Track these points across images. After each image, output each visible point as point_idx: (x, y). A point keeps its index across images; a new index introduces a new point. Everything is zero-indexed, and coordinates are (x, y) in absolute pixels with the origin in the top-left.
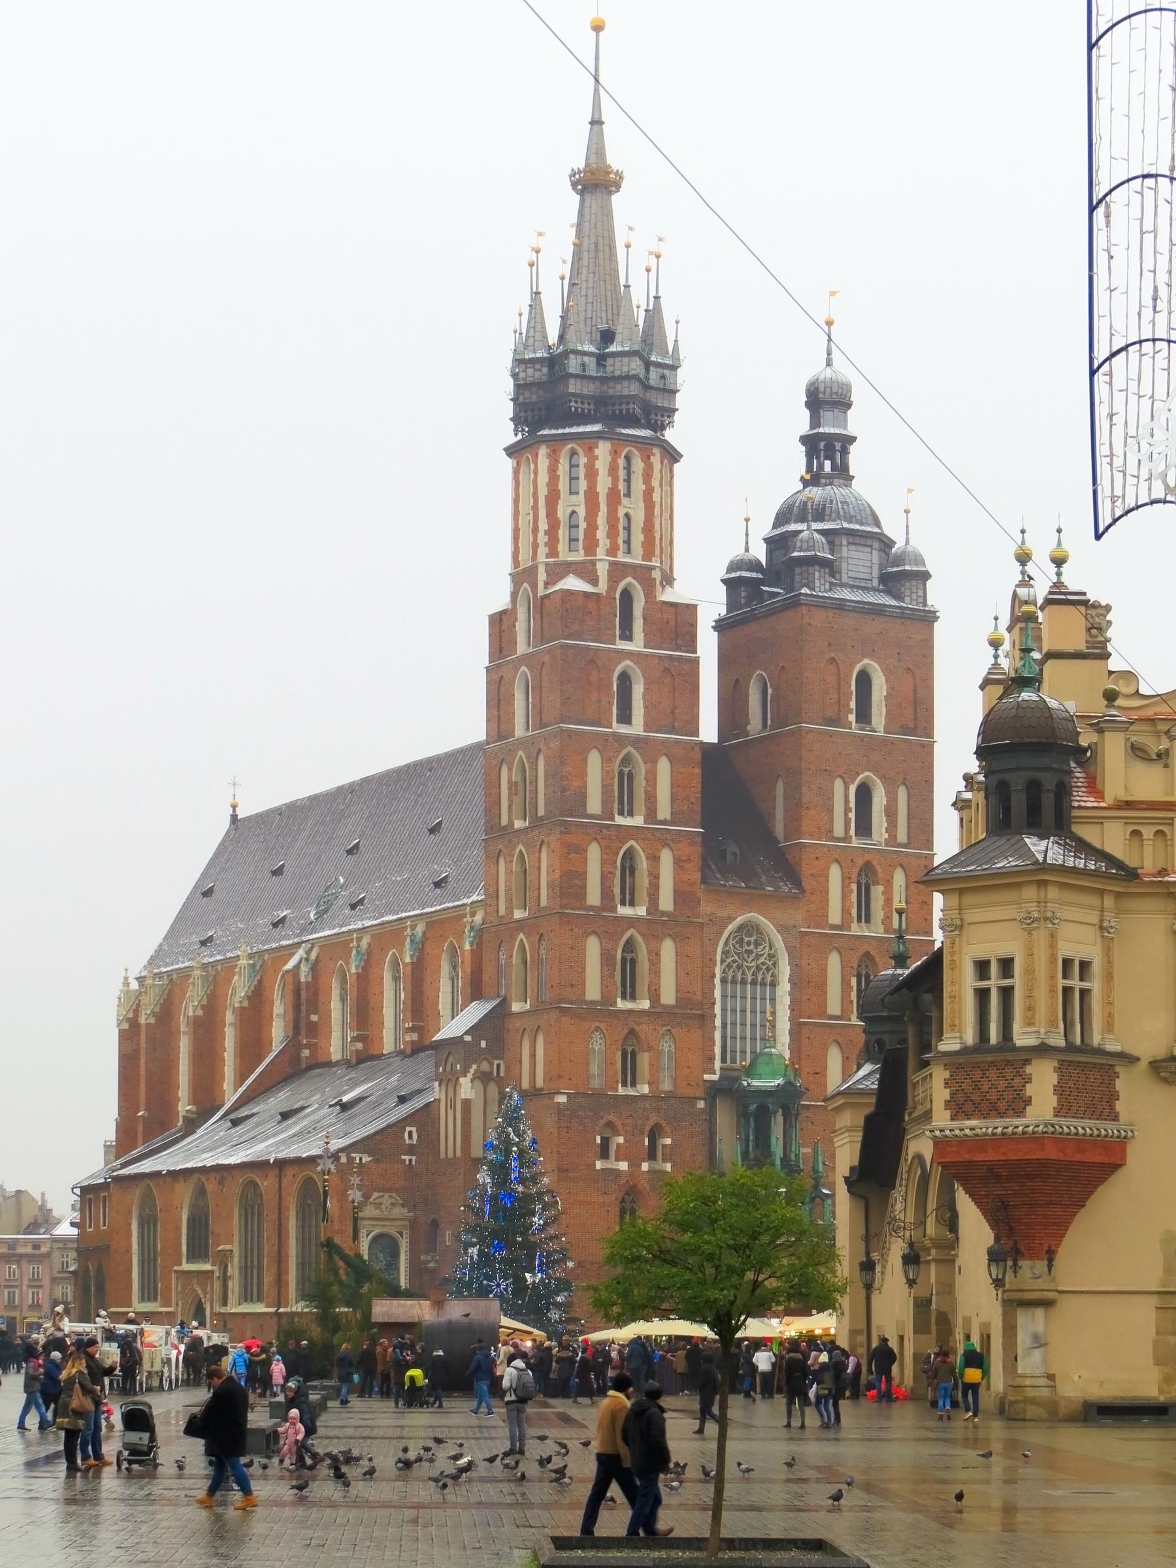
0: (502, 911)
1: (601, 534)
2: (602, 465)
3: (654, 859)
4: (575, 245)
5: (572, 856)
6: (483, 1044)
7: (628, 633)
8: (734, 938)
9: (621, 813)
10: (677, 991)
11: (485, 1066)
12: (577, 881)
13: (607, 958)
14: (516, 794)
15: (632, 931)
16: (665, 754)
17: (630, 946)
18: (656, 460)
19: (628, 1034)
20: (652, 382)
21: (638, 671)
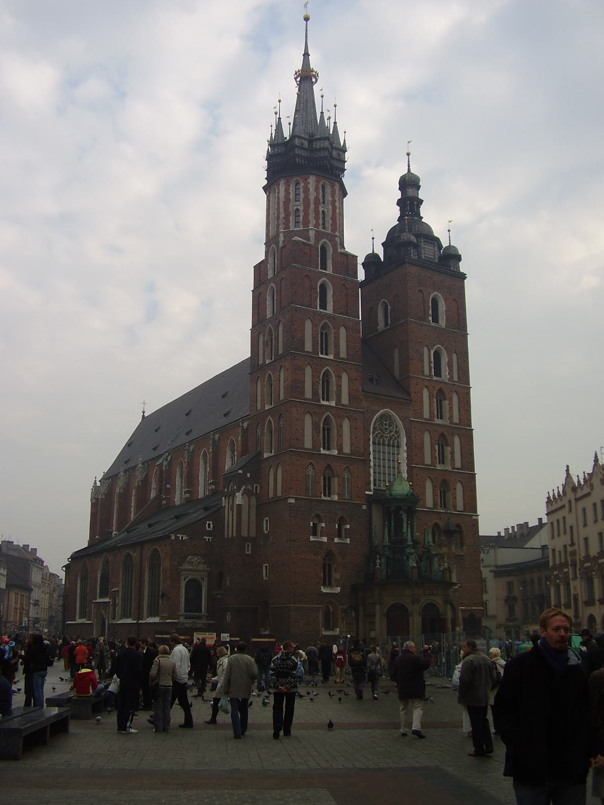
0: (259, 407)
1: (311, 217)
2: (311, 187)
4: (298, 94)
5: (297, 371)
6: (249, 475)
7: (324, 266)
8: (379, 421)
9: (322, 354)
10: (351, 446)
11: (249, 487)
13: (315, 426)
14: (267, 347)
15: (328, 413)
16: (344, 325)
17: (327, 421)
18: (337, 188)
19: (326, 467)
21: (330, 284)
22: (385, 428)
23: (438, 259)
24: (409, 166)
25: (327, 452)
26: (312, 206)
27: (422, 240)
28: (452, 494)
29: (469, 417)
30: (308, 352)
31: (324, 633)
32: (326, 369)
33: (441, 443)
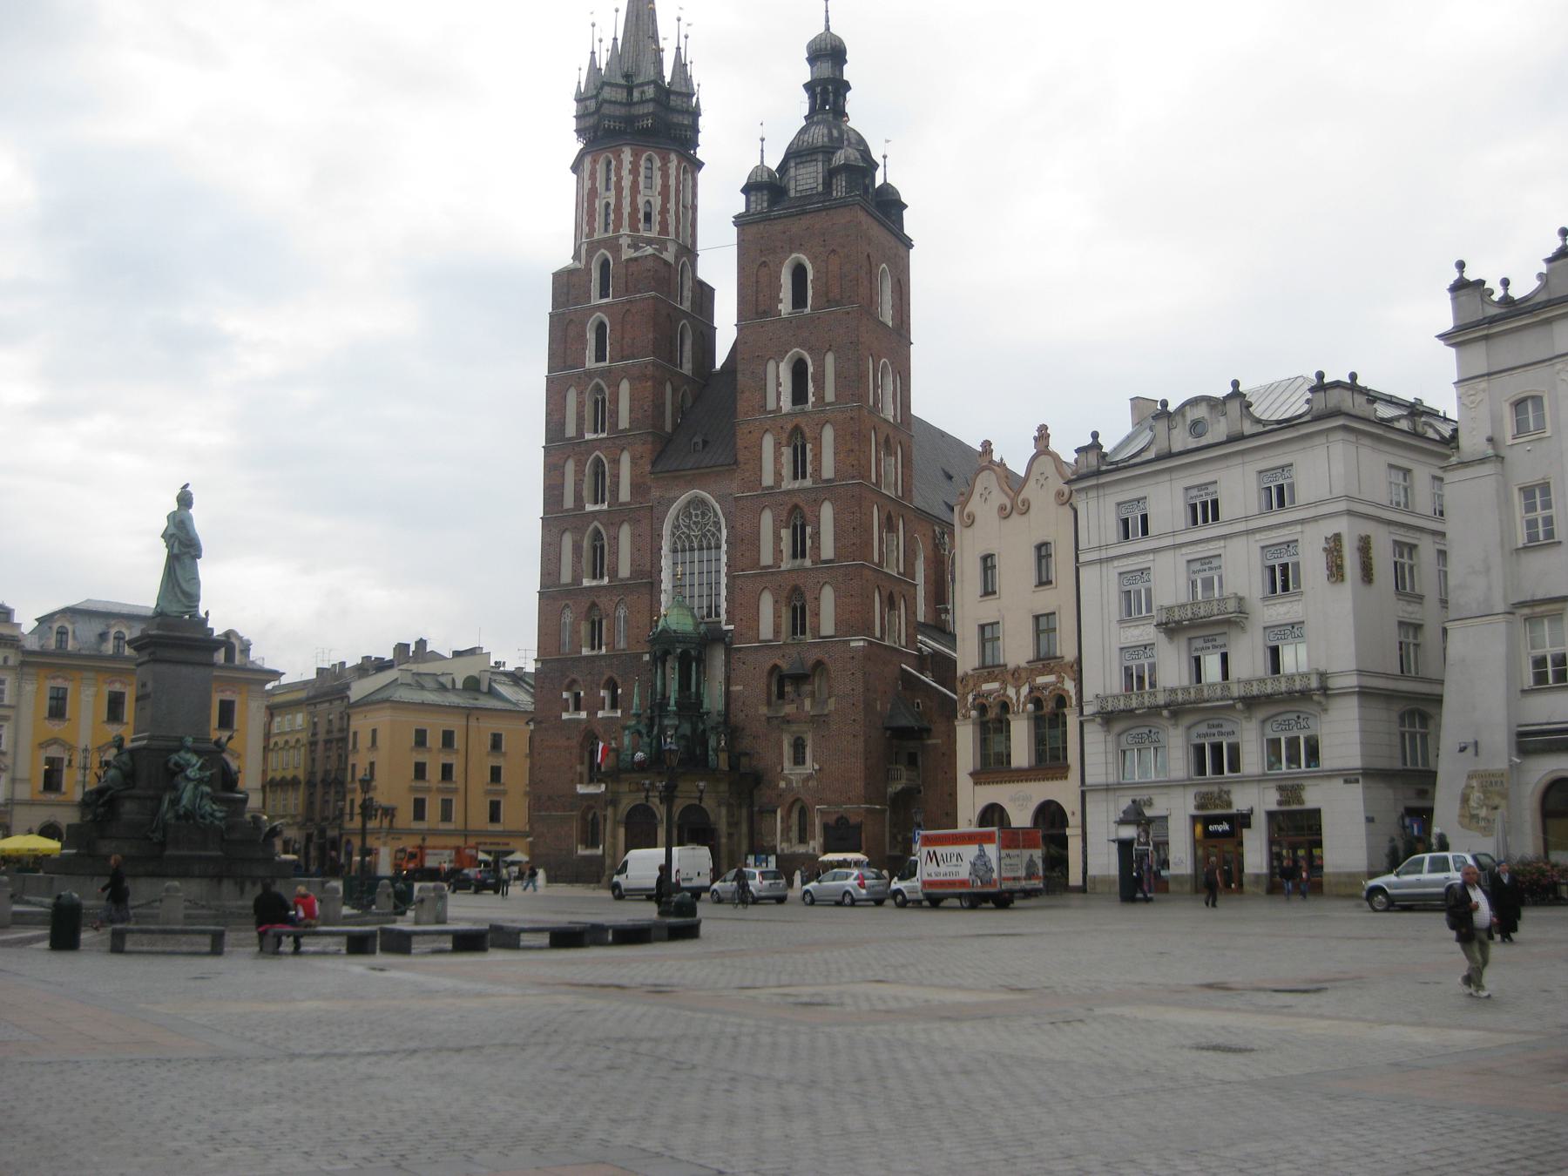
2: (586, 175)
3: (616, 462)
9: (596, 431)
10: (631, 565)
12: (556, 492)
15: (596, 523)
17: (597, 533)
20: (635, 99)
22: (695, 523)
23: (824, 183)
24: (827, 21)
25: (594, 583)
26: (586, 205)
27: (793, 164)
28: (811, 612)
29: (853, 463)
30: (570, 439)
31: (582, 851)
32: (594, 455)
33: (798, 523)
